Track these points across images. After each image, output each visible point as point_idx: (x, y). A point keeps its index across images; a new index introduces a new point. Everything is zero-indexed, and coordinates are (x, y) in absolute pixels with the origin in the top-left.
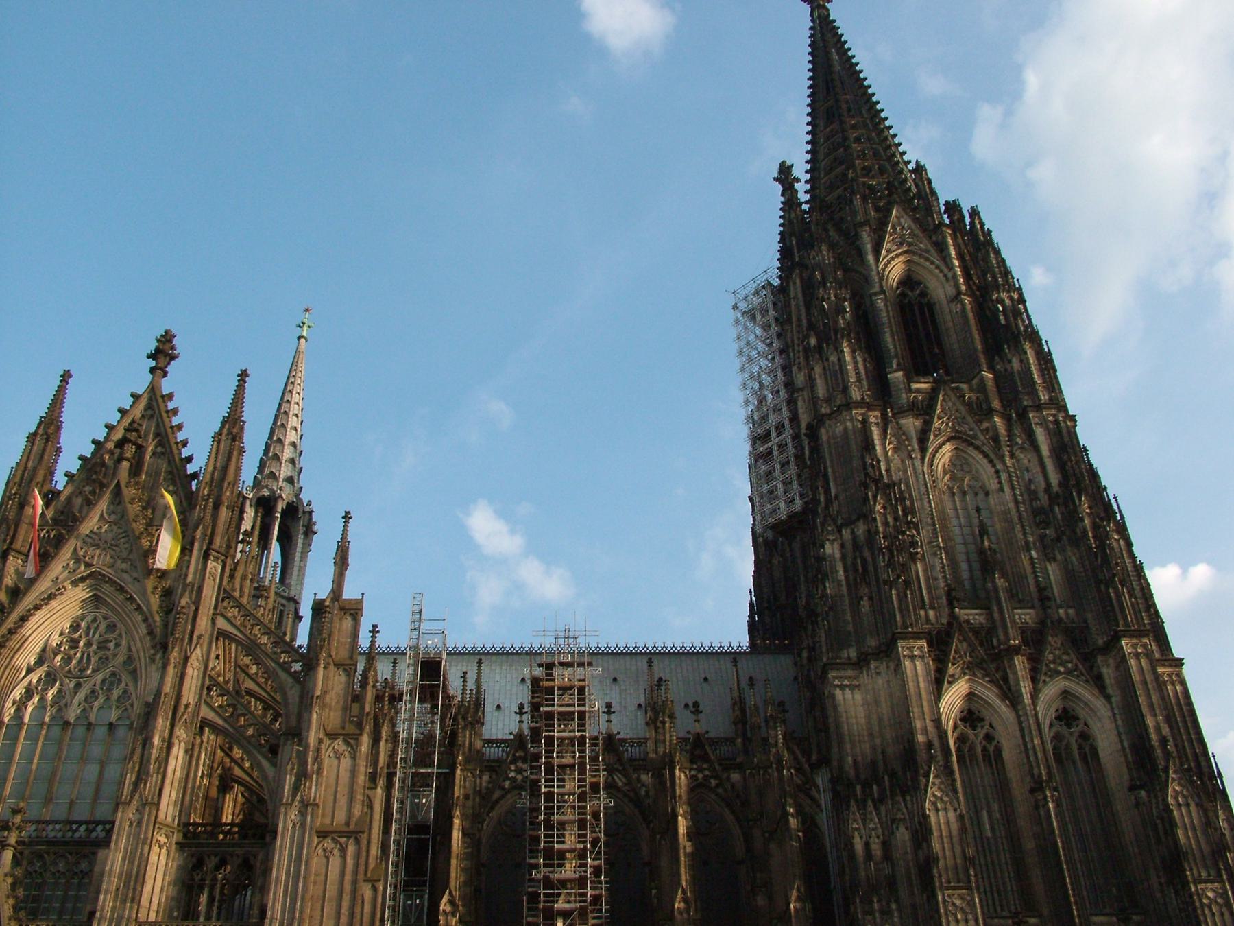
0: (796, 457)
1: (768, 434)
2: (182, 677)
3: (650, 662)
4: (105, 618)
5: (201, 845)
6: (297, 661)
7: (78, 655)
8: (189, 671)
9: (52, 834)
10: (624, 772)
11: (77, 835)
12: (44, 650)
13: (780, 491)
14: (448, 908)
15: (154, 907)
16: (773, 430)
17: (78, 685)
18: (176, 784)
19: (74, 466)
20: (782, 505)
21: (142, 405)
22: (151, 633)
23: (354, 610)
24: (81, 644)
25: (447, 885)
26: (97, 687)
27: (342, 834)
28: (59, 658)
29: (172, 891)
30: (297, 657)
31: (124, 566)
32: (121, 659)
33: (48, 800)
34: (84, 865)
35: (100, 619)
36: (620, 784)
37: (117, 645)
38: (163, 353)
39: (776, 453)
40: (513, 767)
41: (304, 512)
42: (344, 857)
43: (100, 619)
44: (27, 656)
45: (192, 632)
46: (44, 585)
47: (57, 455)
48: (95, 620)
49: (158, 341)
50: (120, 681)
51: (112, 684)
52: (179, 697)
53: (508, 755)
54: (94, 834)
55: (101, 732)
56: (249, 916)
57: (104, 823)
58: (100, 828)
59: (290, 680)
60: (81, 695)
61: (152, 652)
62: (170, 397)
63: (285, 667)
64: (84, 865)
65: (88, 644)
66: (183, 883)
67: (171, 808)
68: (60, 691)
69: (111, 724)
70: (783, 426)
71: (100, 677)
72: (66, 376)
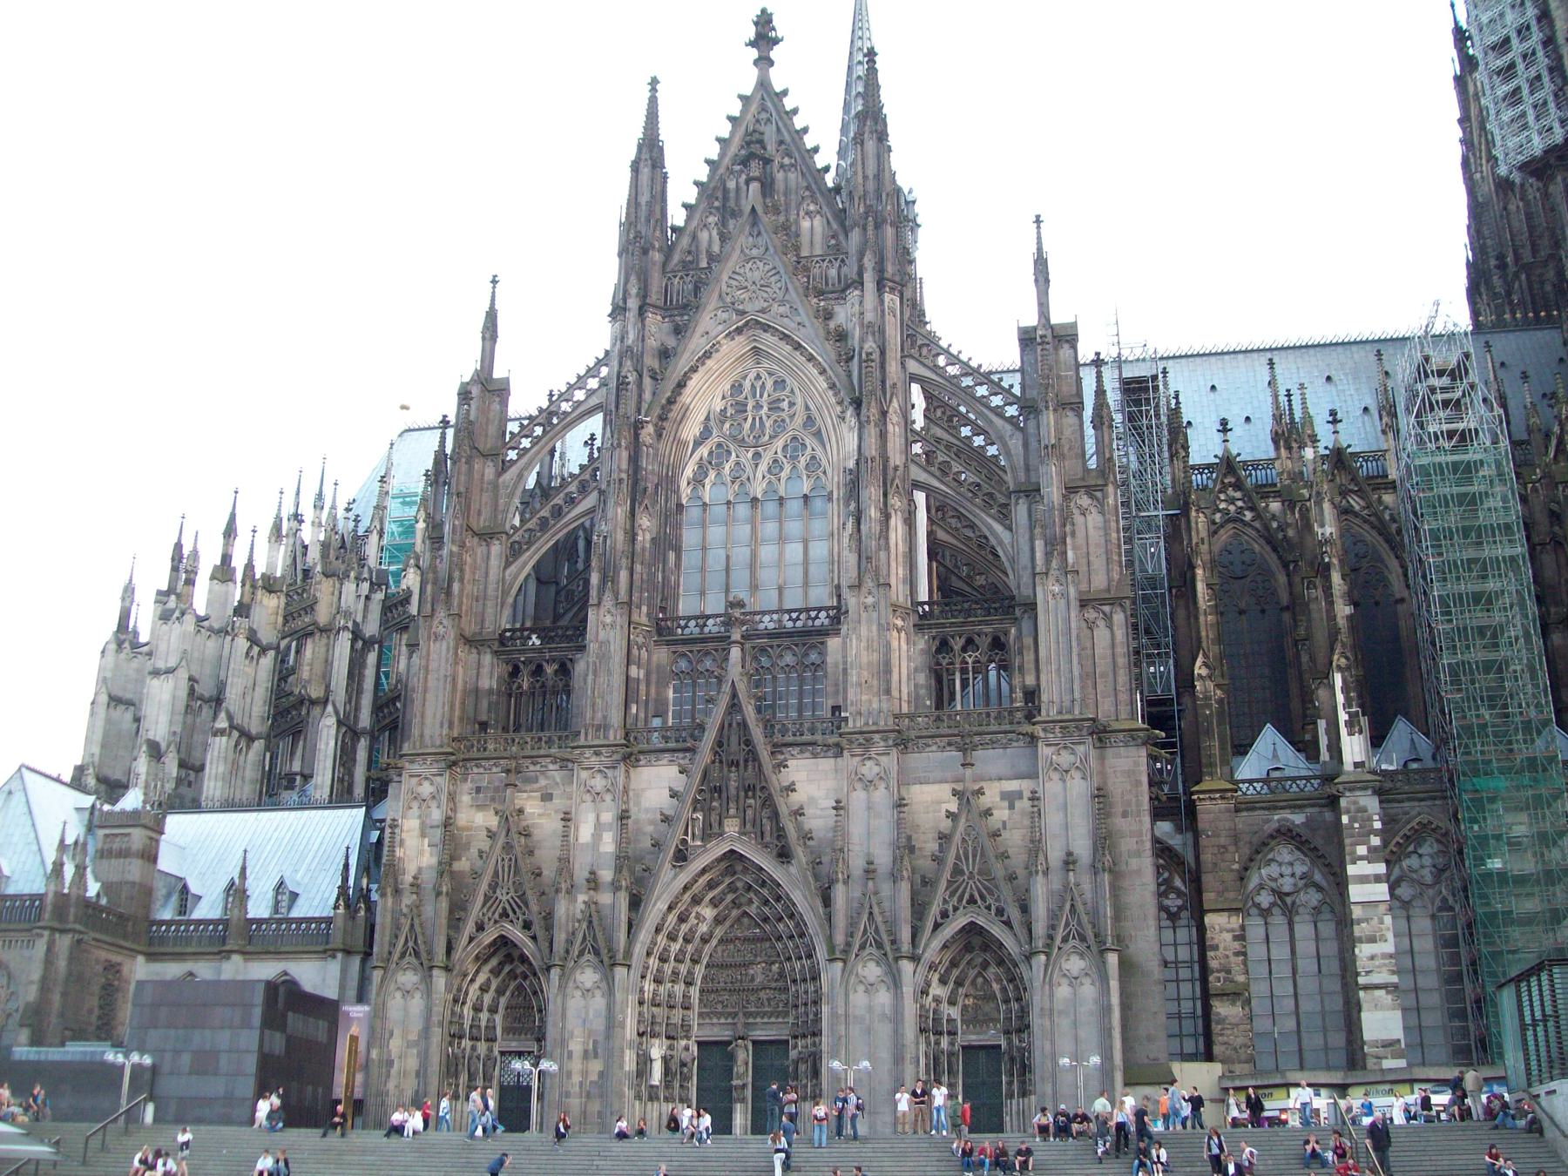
0: (1551, 70)
1: (1507, 40)
2: (883, 436)
3: (1379, 354)
4: (770, 374)
5: (943, 625)
6: (1011, 404)
7: (750, 420)
8: (890, 428)
9: (771, 626)
10: (1360, 492)
11: (799, 624)
12: (707, 418)
13: (1531, 118)
14: (1204, 672)
15: (905, 697)
16: (1513, 35)
17: (757, 455)
18: (900, 559)
19: (692, 196)
20: (1536, 140)
21: (754, 108)
22: (832, 386)
23: (1066, 337)
24: (749, 407)
25: (1199, 647)
26: (780, 455)
27: (1103, 601)
28: (727, 425)
29: (922, 678)
30: (1011, 399)
31: (782, 309)
32: (799, 420)
33: (754, 587)
34: (813, 657)
35: (764, 375)
36: (1357, 508)
37: (792, 404)
38: (764, 37)
39: (1521, 67)
40: (1222, 497)
41: (907, 203)
42: (1110, 627)
43: (764, 375)
44: (691, 430)
45: (883, 382)
46: (696, 344)
47: (665, 182)
48: (758, 377)
49: (756, 24)
50: (804, 445)
51: (795, 450)
52: (885, 459)
53: (1215, 481)
54: (817, 622)
55: (794, 506)
56: (1012, 701)
57: (827, 609)
58: (823, 614)
59: (1008, 427)
60: (763, 467)
61: (839, 409)
62: (785, 93)
63: (998, 411)
64: (813, 657)
65: (758, 406)
66: (930, 669)
67: (901, 587)
68: (738, 463)
69: (805, 497)
70: (1528, 28)
71: (779, 444)
72: (654, 82)
